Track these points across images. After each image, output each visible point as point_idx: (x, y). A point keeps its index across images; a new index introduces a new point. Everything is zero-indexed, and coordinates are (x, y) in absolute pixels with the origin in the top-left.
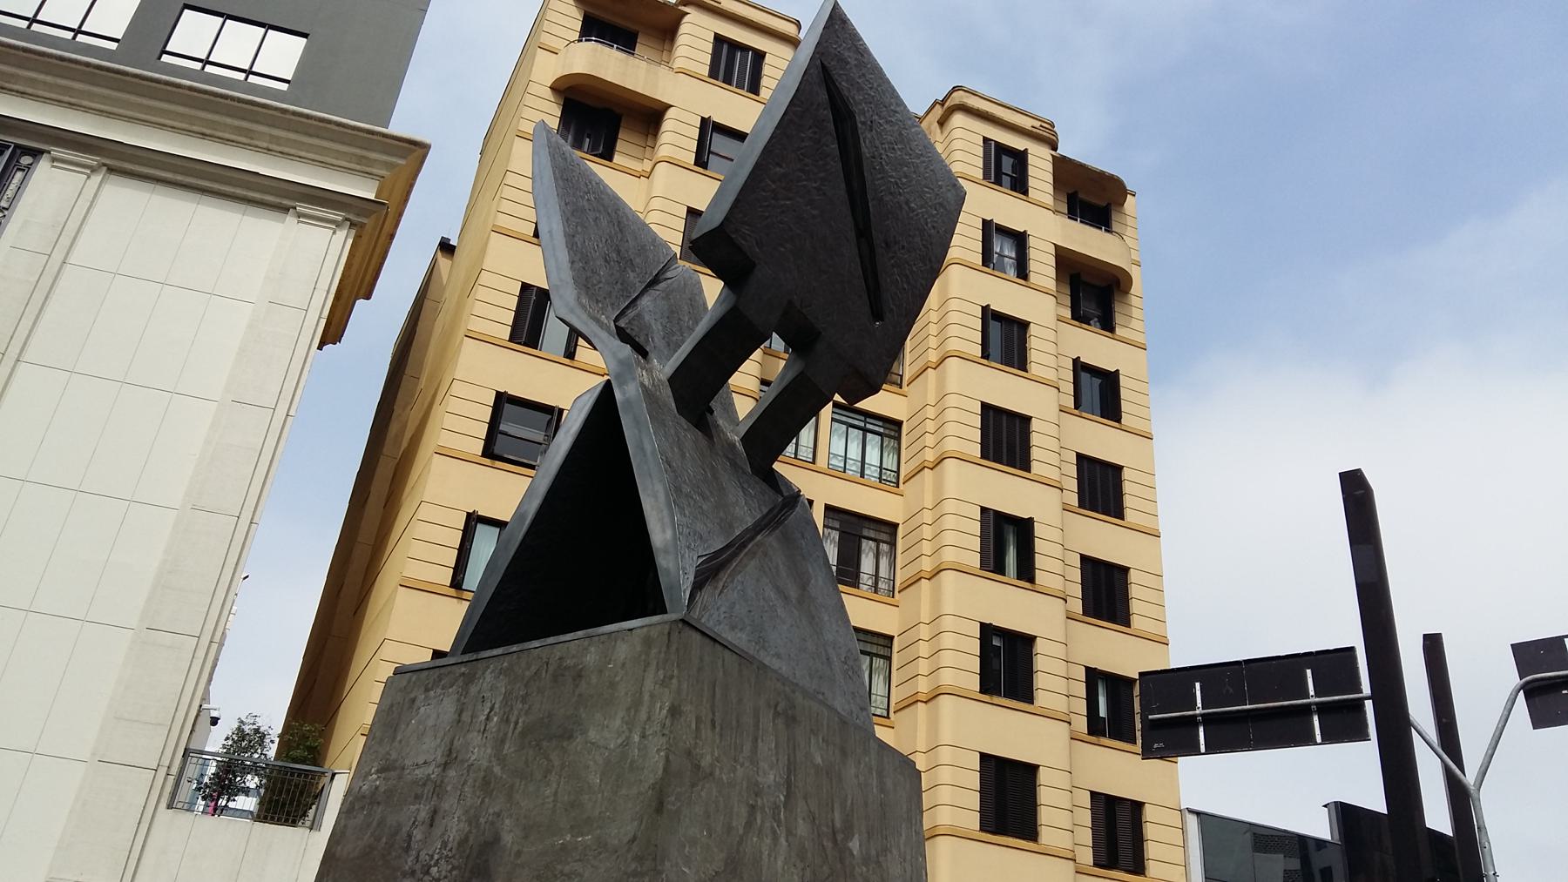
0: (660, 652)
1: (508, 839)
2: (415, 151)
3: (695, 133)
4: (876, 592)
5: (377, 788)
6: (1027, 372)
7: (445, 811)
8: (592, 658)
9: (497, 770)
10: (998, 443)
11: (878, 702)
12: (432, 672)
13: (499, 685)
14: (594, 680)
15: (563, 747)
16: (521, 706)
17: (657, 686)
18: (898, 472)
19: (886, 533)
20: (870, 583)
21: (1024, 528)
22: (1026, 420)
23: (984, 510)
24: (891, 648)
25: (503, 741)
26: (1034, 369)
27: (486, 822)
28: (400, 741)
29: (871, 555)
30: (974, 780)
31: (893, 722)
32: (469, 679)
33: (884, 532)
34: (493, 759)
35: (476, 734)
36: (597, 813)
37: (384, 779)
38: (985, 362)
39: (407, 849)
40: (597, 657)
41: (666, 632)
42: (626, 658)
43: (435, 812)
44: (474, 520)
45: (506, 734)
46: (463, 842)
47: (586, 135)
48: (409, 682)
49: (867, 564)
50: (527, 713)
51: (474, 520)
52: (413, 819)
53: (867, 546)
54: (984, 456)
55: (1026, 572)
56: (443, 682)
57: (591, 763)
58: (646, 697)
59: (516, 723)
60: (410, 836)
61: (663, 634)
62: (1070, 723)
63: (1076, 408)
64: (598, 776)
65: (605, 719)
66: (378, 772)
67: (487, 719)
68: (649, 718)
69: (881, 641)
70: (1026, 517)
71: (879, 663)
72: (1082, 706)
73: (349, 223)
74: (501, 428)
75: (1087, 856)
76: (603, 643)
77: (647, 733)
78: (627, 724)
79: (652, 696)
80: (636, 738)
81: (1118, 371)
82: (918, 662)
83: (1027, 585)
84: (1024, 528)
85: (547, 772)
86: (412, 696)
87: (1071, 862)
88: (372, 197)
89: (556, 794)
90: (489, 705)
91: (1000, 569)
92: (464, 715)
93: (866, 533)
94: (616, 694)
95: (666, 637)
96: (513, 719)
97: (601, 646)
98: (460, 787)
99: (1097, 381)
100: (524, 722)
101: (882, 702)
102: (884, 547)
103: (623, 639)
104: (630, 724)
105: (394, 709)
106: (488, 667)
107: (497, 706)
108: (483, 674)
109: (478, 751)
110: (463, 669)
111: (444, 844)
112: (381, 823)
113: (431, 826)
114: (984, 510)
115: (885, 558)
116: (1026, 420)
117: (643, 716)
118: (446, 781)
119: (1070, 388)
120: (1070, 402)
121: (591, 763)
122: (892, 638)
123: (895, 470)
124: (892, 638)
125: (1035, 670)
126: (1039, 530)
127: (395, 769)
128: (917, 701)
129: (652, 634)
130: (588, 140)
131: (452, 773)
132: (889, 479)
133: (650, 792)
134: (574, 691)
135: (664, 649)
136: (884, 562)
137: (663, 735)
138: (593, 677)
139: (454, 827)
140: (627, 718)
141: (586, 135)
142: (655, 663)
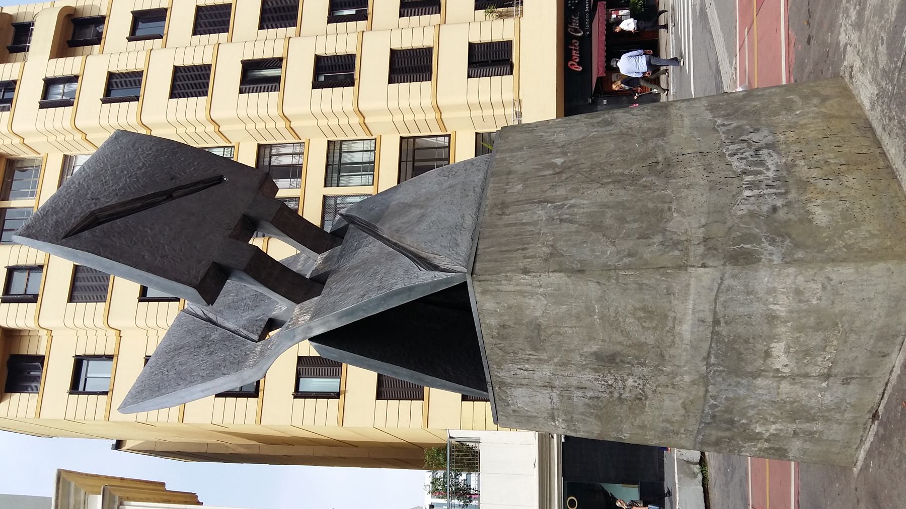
0: (491, 284)
1: (595, 348)
2: (64, 478)
3: (14, 306)
4: (303, 154)
5: (563, 420)
6: (143, 71)
7: (578, 382)
8: (493, 321)
9: (556, 360)
10: (195, 86)
11: (368, 146)
12: (497, 404)
13: (507, 368)
14: (506, 318)
15: (545, 328)
16: (520, 354)
17: (511, 283)
18: (224, 147)
19: (265, 151)
20: (297, 158)
21: (249, 67)
22: (176, 69)
23: (241, 92)
24: (335, 141)
25: (540, 360)
26: (140, 67)
27: (585, 360)
28: (538, 413)
29: (280, 159)
30: (404, 86)
31: (378, 136)
32: (503, 384)
33: (265, 152)
34: (550, 364)
35: (535, 375)
36: (582, 304)
37: (558, 417)
38: (141, 99)
39: (598, 398)
40: (493, 318)
41: (479, 283)
42: (494, 303)
43: (578, 388)
44: (298, 394)
45: (536, 359)
46: (596, 370)
47: (29, 375)
48: (502, 415)
49: (286, 161)
50: (525, 350)
51: (298, 394)
52: (582, 398)
53: (275, 161)
54: (205, 94)
55: (277, 63)
56: (504, 398)
57: (554, 312)
58: (518, 288)
59: (530, 355)
60: (591, 398)
61: (480, 284)
62: (363, 31)
63: (162, 37)
64: (562, 307)
65: (530, 308)
66: (554, 421)
67: (526, 370)
68: (530, 285)
69: (331, 147)
70: (241, 65)
71: (345, 148)
72: (352, 24)
73: (120, 506)
74: (238, 390)
75: (435, 18)
76: (484, 317)
77: (539, 284)
78: (533, 296)
79: (517, 285)
80: (542, 290)
81: (132, 12)
82: (352, 124)
83: (284, 62)
84: (249, 67)
85: (559, 334)
86: (511, 412)
87: (441, 26)
88: (100, 497)
89: (571, 327)
90: (518, 371)
91: (277, 80)
92: (524, 383)
93: (267, 163)
94: (515, 304)
95: (482, 283)
96: (527, 357)
97: (485, 317)
98: (565, 378)
99: (141, 25)
100: (530, 351)
101: (367, 144)
102: (274, 151)
103: (483, 306)
104: (532, 294)
105: (518, 420)
106: (496, 375)
107: (519, 367)
108: (500, 377)
109: (546, 371)
110: (497, 388)
111: (596, 379)
112: (582, 414)
113: (585, 388)
114: (241, 92)
115: (280, 150)
116: (176, 69)
117: (529, 288)
118: (560, 385)
119: (149, 43)
120: (158, 42)
121: (554, 312)
122: (329, 142)
123: (223, 149)
124: (329, 142)
125: (335, 54)
126: (248, 57)
127: (553, 413)
128: (364, 123)
129: (479, 291)
130: (31, 373)
131: (557, 383)
132: (230, 152)
133: (572, 278)
134: (513, 328)
135: (489, 283)
136: (283, 150)
137: (540, 276)
138: (505, 318)
139: (587, 377)
140: (530, 297)
141: (29, 375)
142: (498, 286)
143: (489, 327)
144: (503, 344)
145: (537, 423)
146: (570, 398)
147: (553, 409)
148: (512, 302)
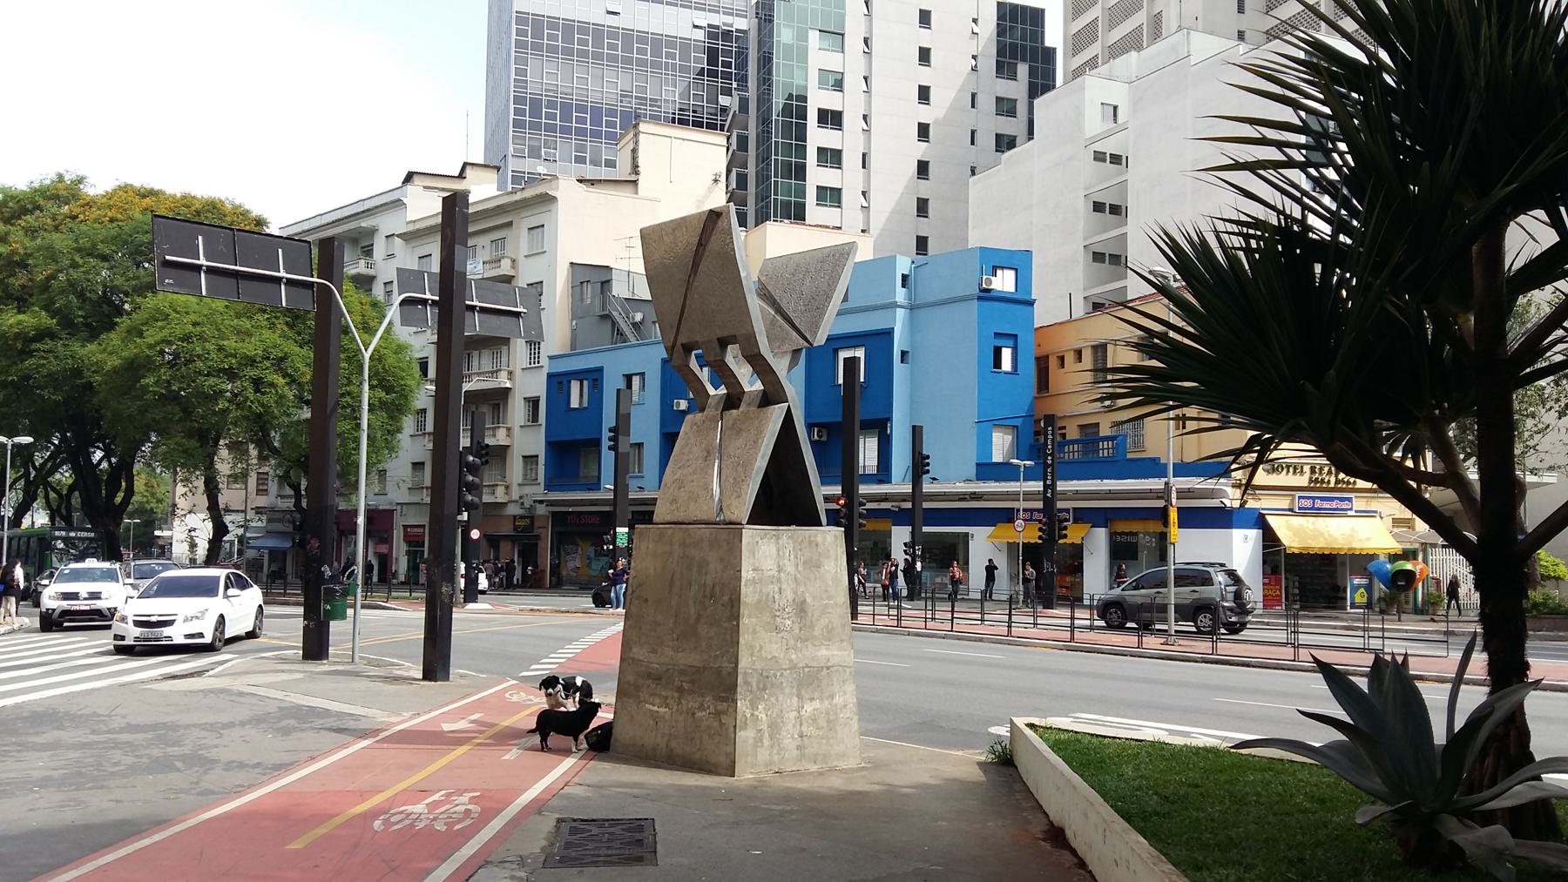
1: (808, 600)
8: (819, 539)
9: (799, 576)
25: (798, 564)
39: (774, 602)
43: (780, 589)
46: (794, 601)
50: (803, 555)
60: (774, 597)
85: (816, 579)
109: (790, 568)
111: (788, 601)
112: (761, 591)
131: (782, 574)
139: (789, 595)
143: (816, 536)
144: (806, 544)
145: (749, 558)
146: (772, 583)
147: (763, 570)
148: (832, 552)
